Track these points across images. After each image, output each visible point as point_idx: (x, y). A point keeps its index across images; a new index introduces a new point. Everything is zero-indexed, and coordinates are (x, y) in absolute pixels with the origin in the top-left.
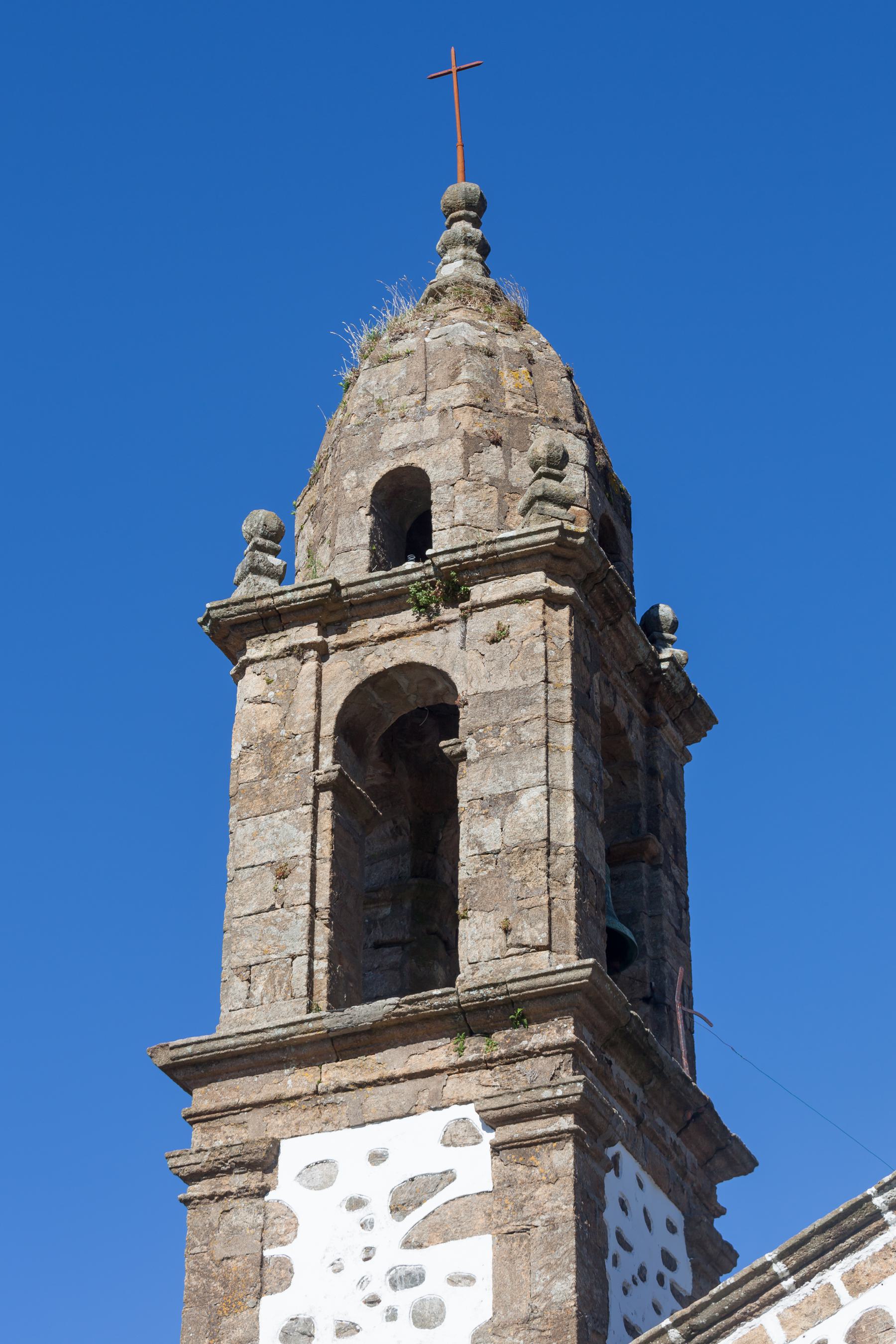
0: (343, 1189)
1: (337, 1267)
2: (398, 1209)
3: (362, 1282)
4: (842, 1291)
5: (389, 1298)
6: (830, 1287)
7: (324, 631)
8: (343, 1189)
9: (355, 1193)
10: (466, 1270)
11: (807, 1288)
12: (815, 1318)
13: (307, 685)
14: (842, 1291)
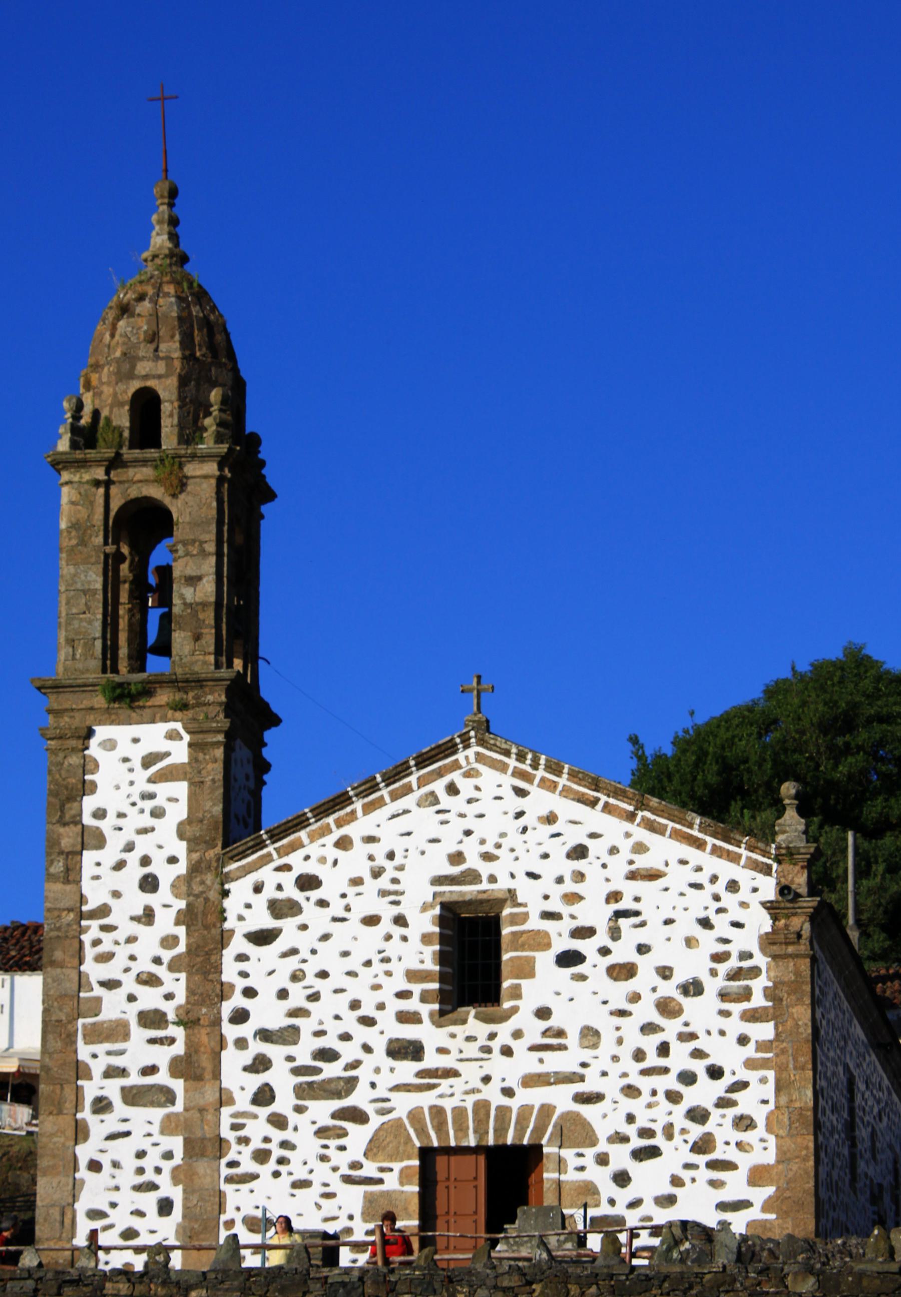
0: (120, 752)
1: (118, 787)
4: (333, 826)
5: (141, 804)
6: (328, 824)
8: (120, 752)
10: (175, 796)
11: (319, 824)
12: (322, 835)
13: (100, 501)
14: (333, 826)
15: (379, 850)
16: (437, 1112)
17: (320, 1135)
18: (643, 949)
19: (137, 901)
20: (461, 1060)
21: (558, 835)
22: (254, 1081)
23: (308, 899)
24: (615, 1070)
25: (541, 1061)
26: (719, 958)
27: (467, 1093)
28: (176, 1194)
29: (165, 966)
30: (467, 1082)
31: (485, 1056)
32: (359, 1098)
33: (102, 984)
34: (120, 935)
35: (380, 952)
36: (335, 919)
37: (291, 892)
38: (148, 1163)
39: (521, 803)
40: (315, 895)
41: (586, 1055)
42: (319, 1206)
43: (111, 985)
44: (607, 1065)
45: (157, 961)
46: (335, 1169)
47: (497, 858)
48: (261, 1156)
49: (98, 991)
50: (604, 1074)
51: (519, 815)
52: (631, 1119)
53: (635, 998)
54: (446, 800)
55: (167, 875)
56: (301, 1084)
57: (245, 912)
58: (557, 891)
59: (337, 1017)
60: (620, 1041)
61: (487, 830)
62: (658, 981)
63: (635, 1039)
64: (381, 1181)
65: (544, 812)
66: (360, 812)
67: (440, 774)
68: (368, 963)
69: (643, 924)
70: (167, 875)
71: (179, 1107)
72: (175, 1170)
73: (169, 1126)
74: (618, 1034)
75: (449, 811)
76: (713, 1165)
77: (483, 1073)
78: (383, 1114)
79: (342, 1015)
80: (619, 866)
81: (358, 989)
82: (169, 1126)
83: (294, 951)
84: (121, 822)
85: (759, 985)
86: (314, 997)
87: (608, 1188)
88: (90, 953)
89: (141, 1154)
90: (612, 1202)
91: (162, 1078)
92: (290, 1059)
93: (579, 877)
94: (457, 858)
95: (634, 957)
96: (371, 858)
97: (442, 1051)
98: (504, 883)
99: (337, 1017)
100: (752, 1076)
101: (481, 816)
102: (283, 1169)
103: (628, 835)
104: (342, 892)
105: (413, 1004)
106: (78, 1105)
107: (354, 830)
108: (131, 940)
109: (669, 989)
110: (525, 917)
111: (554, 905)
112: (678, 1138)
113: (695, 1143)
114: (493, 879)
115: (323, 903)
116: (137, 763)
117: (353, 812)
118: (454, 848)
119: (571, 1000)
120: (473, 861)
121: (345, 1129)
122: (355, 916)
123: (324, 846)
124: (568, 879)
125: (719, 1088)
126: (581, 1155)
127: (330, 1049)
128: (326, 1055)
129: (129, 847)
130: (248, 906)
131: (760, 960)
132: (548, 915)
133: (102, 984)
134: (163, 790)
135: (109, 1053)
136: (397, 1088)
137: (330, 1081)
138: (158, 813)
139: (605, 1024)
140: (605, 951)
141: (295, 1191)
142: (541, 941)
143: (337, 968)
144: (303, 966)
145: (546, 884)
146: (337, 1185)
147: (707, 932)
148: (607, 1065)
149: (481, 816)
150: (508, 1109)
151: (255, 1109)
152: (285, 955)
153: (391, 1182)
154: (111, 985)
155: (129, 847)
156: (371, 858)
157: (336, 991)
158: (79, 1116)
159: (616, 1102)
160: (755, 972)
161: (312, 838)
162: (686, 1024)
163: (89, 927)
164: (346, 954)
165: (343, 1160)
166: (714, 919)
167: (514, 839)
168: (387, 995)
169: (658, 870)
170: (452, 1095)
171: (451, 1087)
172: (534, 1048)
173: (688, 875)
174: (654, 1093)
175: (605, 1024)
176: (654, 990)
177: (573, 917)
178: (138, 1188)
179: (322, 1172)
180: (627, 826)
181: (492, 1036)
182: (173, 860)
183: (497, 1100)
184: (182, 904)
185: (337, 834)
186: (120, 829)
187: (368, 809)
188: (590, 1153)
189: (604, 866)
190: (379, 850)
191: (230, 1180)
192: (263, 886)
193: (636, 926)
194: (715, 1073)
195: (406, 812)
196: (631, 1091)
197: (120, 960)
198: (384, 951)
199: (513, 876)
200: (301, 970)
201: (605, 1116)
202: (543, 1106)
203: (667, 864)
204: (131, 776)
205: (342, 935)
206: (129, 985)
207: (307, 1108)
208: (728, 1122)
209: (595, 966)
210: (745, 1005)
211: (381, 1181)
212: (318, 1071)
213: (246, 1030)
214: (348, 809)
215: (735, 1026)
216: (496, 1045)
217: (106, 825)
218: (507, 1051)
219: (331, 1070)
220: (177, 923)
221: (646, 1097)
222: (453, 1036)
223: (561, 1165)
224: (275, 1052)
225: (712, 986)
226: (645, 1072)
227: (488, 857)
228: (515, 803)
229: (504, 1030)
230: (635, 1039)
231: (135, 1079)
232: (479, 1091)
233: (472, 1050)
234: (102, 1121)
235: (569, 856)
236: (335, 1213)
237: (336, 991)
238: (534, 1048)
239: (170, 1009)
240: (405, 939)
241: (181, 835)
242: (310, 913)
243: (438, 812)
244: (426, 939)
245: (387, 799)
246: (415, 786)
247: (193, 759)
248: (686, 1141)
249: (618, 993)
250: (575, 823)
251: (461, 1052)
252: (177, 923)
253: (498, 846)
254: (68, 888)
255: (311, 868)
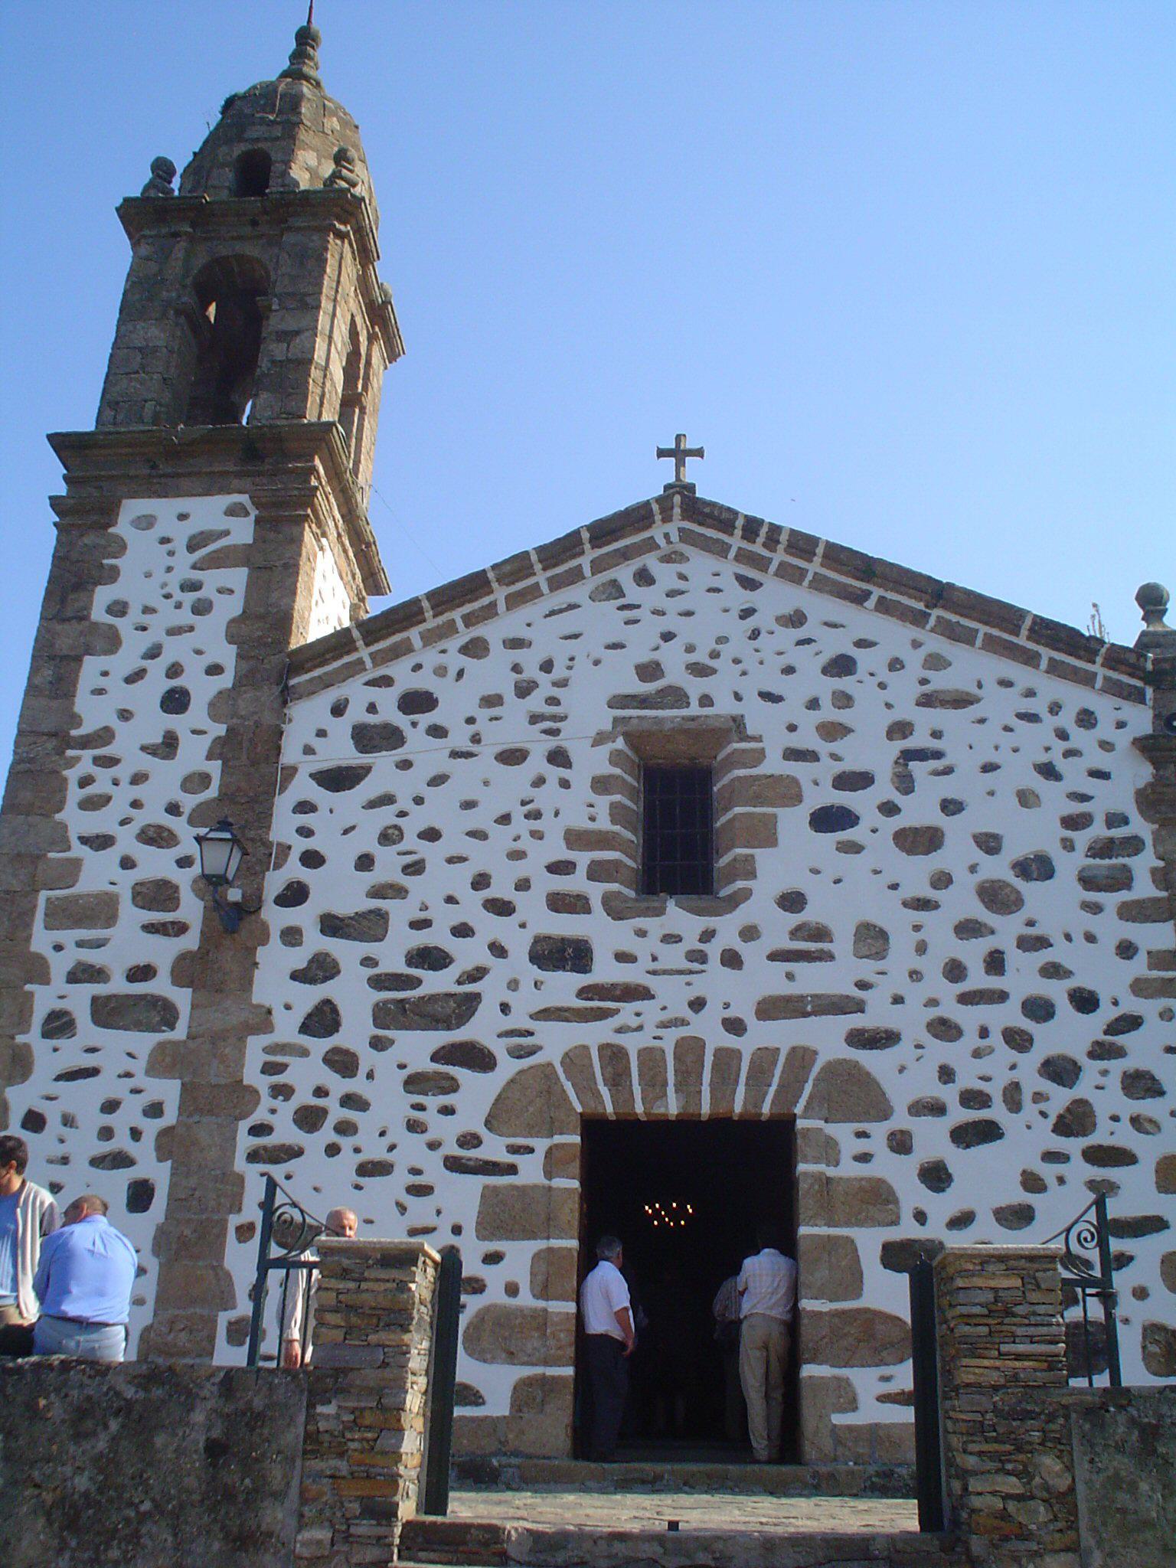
0: (159, 531)
2: (192, 547)
3: (164, 585)
4: (460, 624)
5: (178, 595)
7: (193, 225)
8: (159, 530)
9: (166, 535)
14: (460, 624)
15: (530, 660)
16: (614, 1055)
17: (411, 1088)
18: (952, 807)
19: (153, 724)
20: (654, 973)
21: (809, 641)
22: (307, 997)
23: (414, 724)
24: (915, 994)
25: (790, 976)
26: (1074, 822)
27: (664, 1025)
28: (159, 1174)
29: (184, 818)
30: (664, 1008)
31: (696, 966)
32: (481, 1029)
33: (84, 840)
34: (123, 772)
35: (524, 803)
36: (455, 754)
37: (390, 713)
38: (120, 1122)
39: (746, 598)
40: (425, 719)
41: (867, 969)
42: (402, 1208)
43: (101, 842)
44: (905, 987)
45: (173, 809)
46: (433, 1146)
47: (714, 671)
48: (309, 1119)
49: (78, 850)
50: (898, 1000)
51: (747, 613)
52: (946, 1074)
53: (942, 880)
54: (634, 592)
55: (203, 690)
56: (386, 1002)
57: (317, 743)
58: (809, 721)
59: (451, 900)
60: (921, 948)
61: (700, 633)
62: (979, 856)
63: (946, 945)
64: (512, 1170)
65: (787, 610)
66: (501, 606)
67: (625, 555)
68: (505, 819)
69: (948, 771)
70: (203, 690)
71: (180, 1033)
72: (165, 1133)
73: (163, 1062)
74: (919, 936)
75: (639, 607)
76: (1098, 1156)
77: (692, 994)
78: (519, 1057)
79: (458, 896)
80: (905, 689)
81: (485, 857)
82: (163, 1062)
83: (387, 800)
84: (146, 619)
85: (1143, 864)
86: (415, 868)
87: (911, 1193)
88: (74, 794)
89: (111, 1106)
90: (921, 1217)
91: (161, 986)
92: (368, 962)
93: (844, 700)
94: (649, 671)
95: (938, 819)
96: (516, 668)
97: (623, 957)
98: (724, 706)
99: (451, 900)
100: (1148, 1008)
101: (689, 614)
102: (346, 1143)
103: (916, 644)
104: (469, 715)
105: (576, 883)
106: (23, 1022)
107: (493, 632)
108: (138, 779)
109: (997, 869)
110: (759, 756)
111: (810, 738)
112: (1030, 1109)
113: (1060, 1117)
114: (706, 701)
115: (437, 731)
116: (180, 544)
117: (493, 605)
118: (645, 657)
119: (837, 881)
120: (675, 674)
121: (453, 1079)
122: (487, 752)
123: (443, 652)
124: (826, 701)
125: (1093, 1026)
126: (862, 1135)
127: (436, 948)
128: (432, 958)
129: (154, 653)
130: (321, 733)
131: (1140, 827)
132: (794, 755)
133: (84, 840)
134: (212, 579)
135: (80, 944)
136: (546, 1014)
137: (433, 998)
138: (202, 608)
139: (897, 922)
140: (889, 809)
141: (362, 1181)
142: (788, 792)
143: (454, 826)
144: (400, 821)
145: (793, 709)
146: (434, 1172)
147: (1052, 784)
148: (905, 987)
149: (689, 614)
150: (736, 1054)
151: (306, 1041)
152: (372, 805)
153: (531, 1171)
154: (101, 842)
155: (154, 653)
156: (516, 668)
157: (451, 860)
158: (20, 1039)
159: (918, 1047)
160: (1134, 845)
161: (428, 639)
162: (1031, 923)
163: (78, 759)
164: (468, 805)
165: (447, 1130)
166: (1061, 765)
167: (739, 645)
168: (533, 867)
169: (967, 694)
170: (640, 1028)
171: (638, 1014)
172: (775, 956)
173: (1013, 702)
174: (984, 1033)
175: (897, 922)
176: (973, 869)
177: (835, 757)
178: (97, 1162)
179: (411, 1151)
180: (913, 632)
181: (707, 936)
182: (215, 670)
183: (716, 1038)
184: (220, 730)
185: (465, 636)
186: (144, 629)
187: (514, 601)
188: (880, 1131)
189: (882, 686)
190: (530, 660)
191: (253, 1157)
192: (346, 707)
193: (937, 773)
194: (1085, 1001)
195: (572, 607)
196: (945, 1029)
197: (119, 806)
198: (532, 801)
199: (738, 697)
200: (396, 827)
201: (902, 1069)
202: (794, 1049)
203: (980, 686)
204: (170, 561)
205: (465, 777)
206: (127, 842)
207: (392, 1042)
208: (1114, 1082)
209: (874, 831)
210: (1124, 896)
211: (512, 1170)
212: (415, 983)
213: (304, 916)
214: (485, 601)
215: (1111, 928)
216: (714, 950)
217: (124, 625)
218: (732, 960)
219: (436, 982)
220: (210, 757)
221: (971, 1040)
222: (641, 933)
223: (830, 1151)
224: (346, 951)
225: (1068, 866)
226: (966, 999)
227: (699, 670)
228: (743, 598)
229: (728, 928)
230: (946, 945)
231: (117, 985)
232: (683, 1022)
233: (674, 957)
234: (55, 1050)
235: (826, 671)
236: (430, 1221)
237: (451, 860)
238: (775, 956)
239: (184, 879)
240: (565, 784)
241: (231, 639)
242: (416, 741)
243: (621, 608)
244: (601, 785)
245: (544, 587)
246: (587, 570)
247: (258, 538)
248: (1043, 1114)
249: (916, 871)
250: (835, 626)
251: (654, 959)
252: (210, 757)
253: (715, 655)
254: (54, 704)
255: (423, 682)
